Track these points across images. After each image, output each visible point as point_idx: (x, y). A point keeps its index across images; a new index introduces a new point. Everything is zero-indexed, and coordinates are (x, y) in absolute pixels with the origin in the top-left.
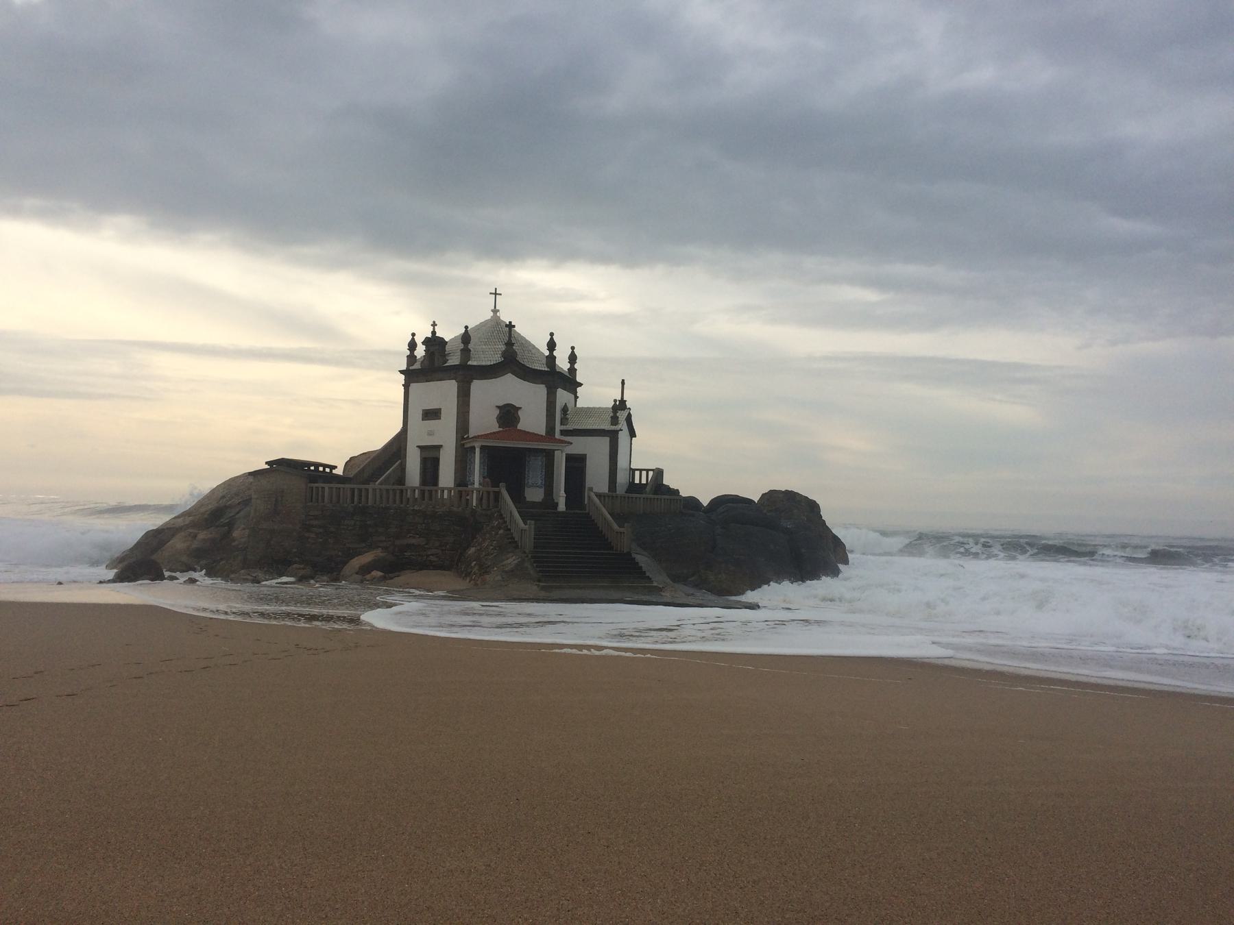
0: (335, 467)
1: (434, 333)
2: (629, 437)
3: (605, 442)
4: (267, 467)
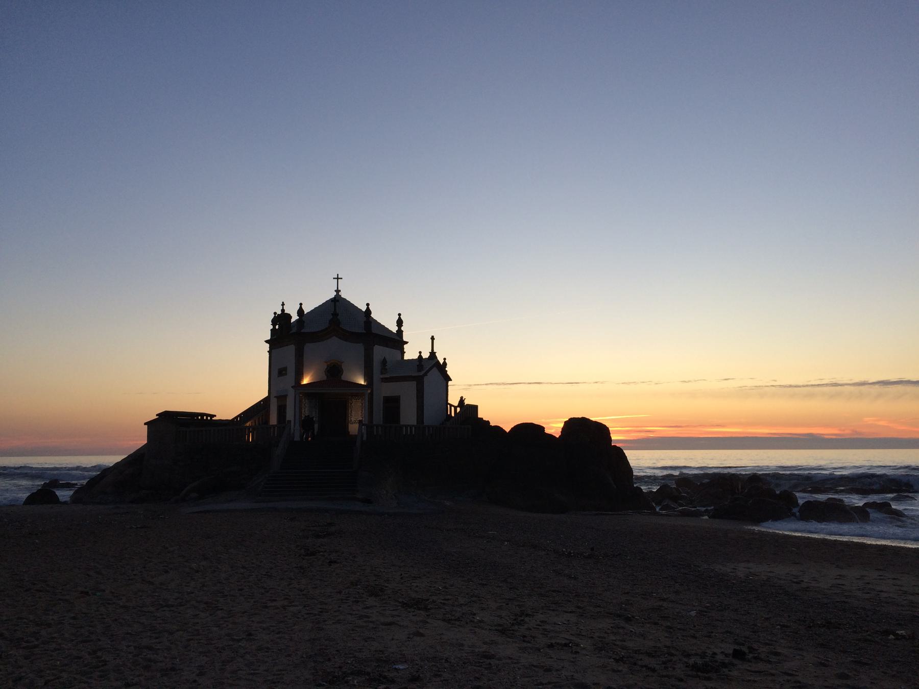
0: (215, 416)
1: (283, 310)
2: (445, 382)
3: (413, 385)
4: (158, 417)
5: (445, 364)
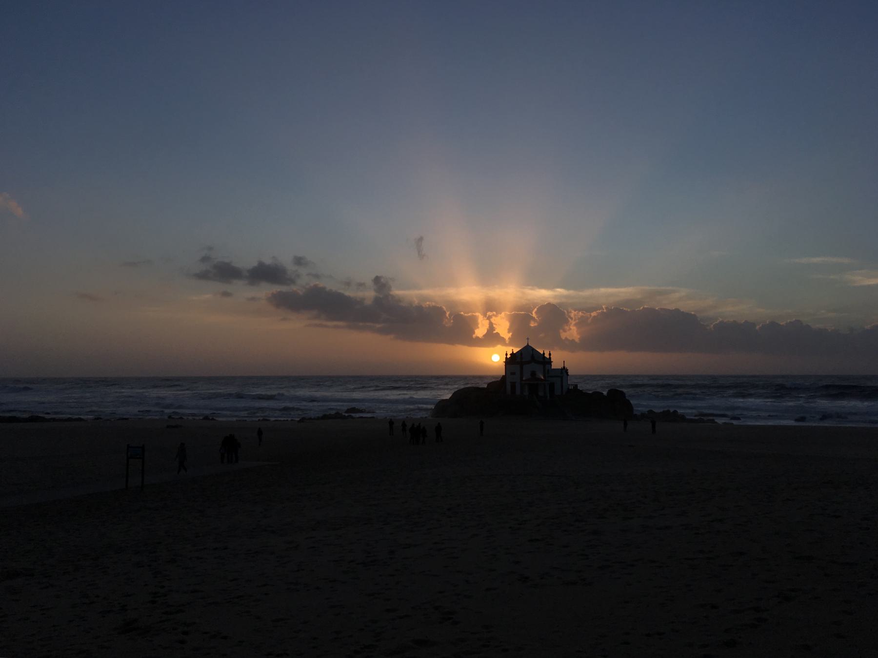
1: (513, 352)
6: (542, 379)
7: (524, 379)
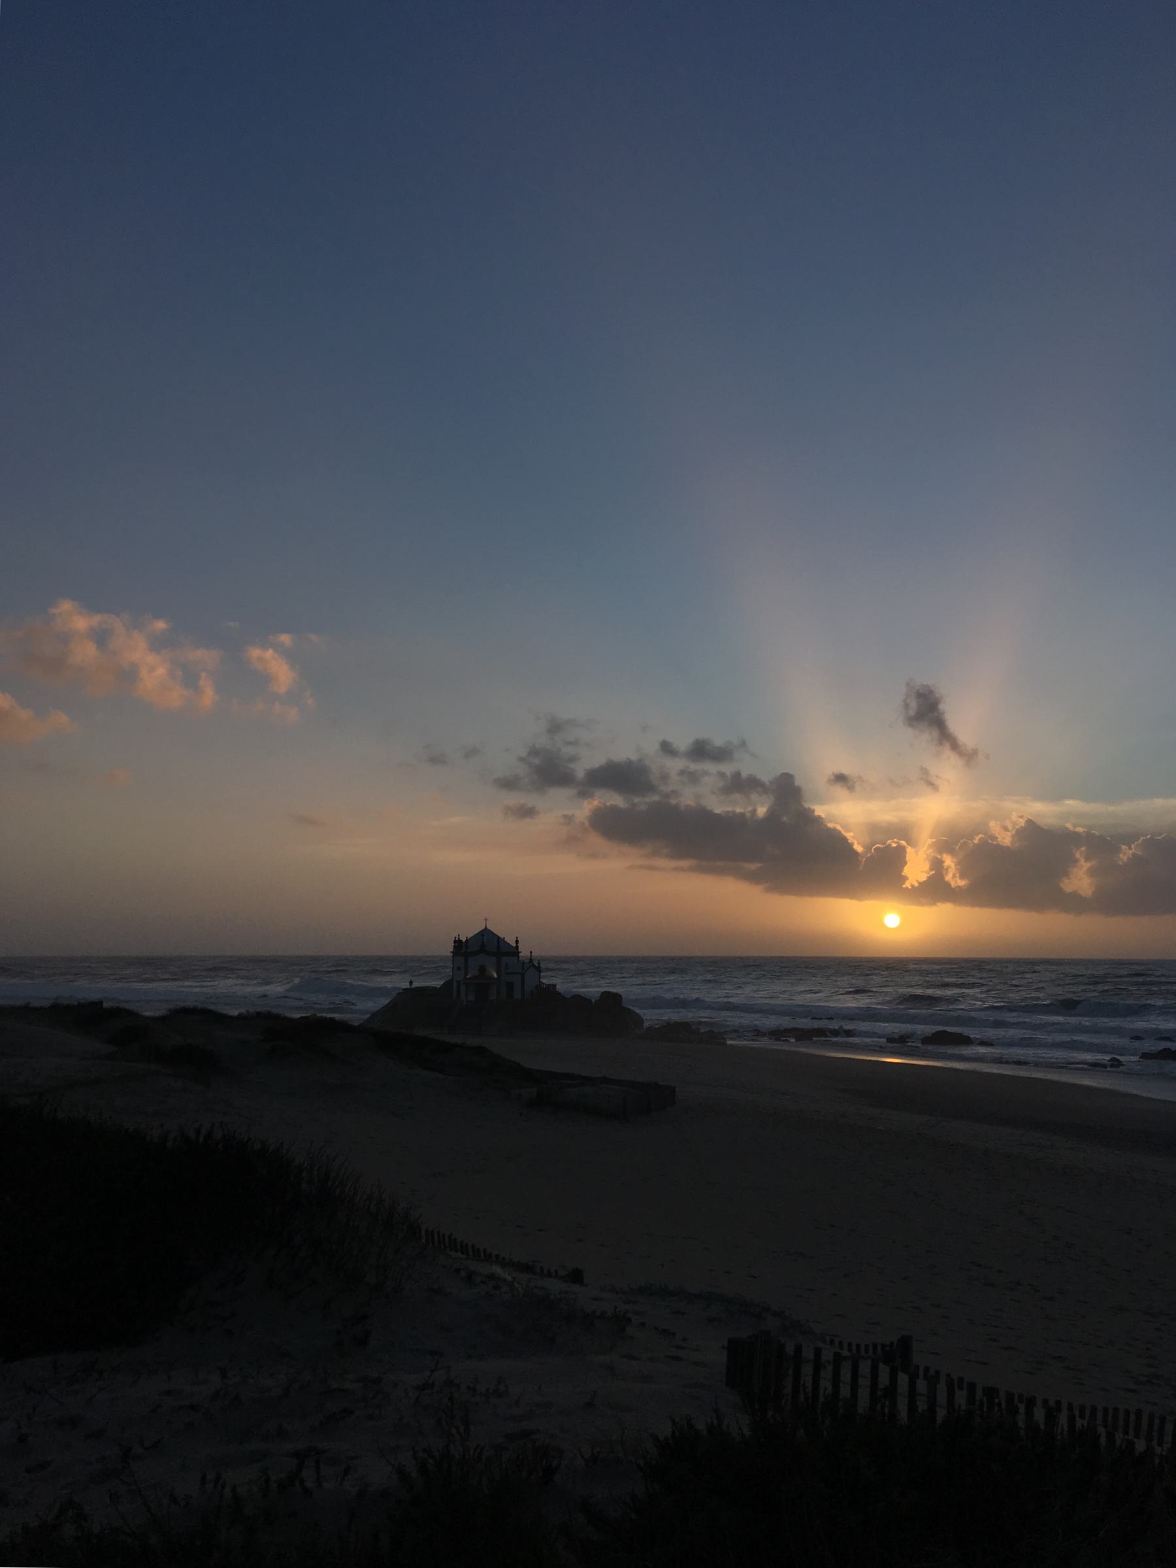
5: (539, 964)
6: (494, 978)
7: (468, 976)
